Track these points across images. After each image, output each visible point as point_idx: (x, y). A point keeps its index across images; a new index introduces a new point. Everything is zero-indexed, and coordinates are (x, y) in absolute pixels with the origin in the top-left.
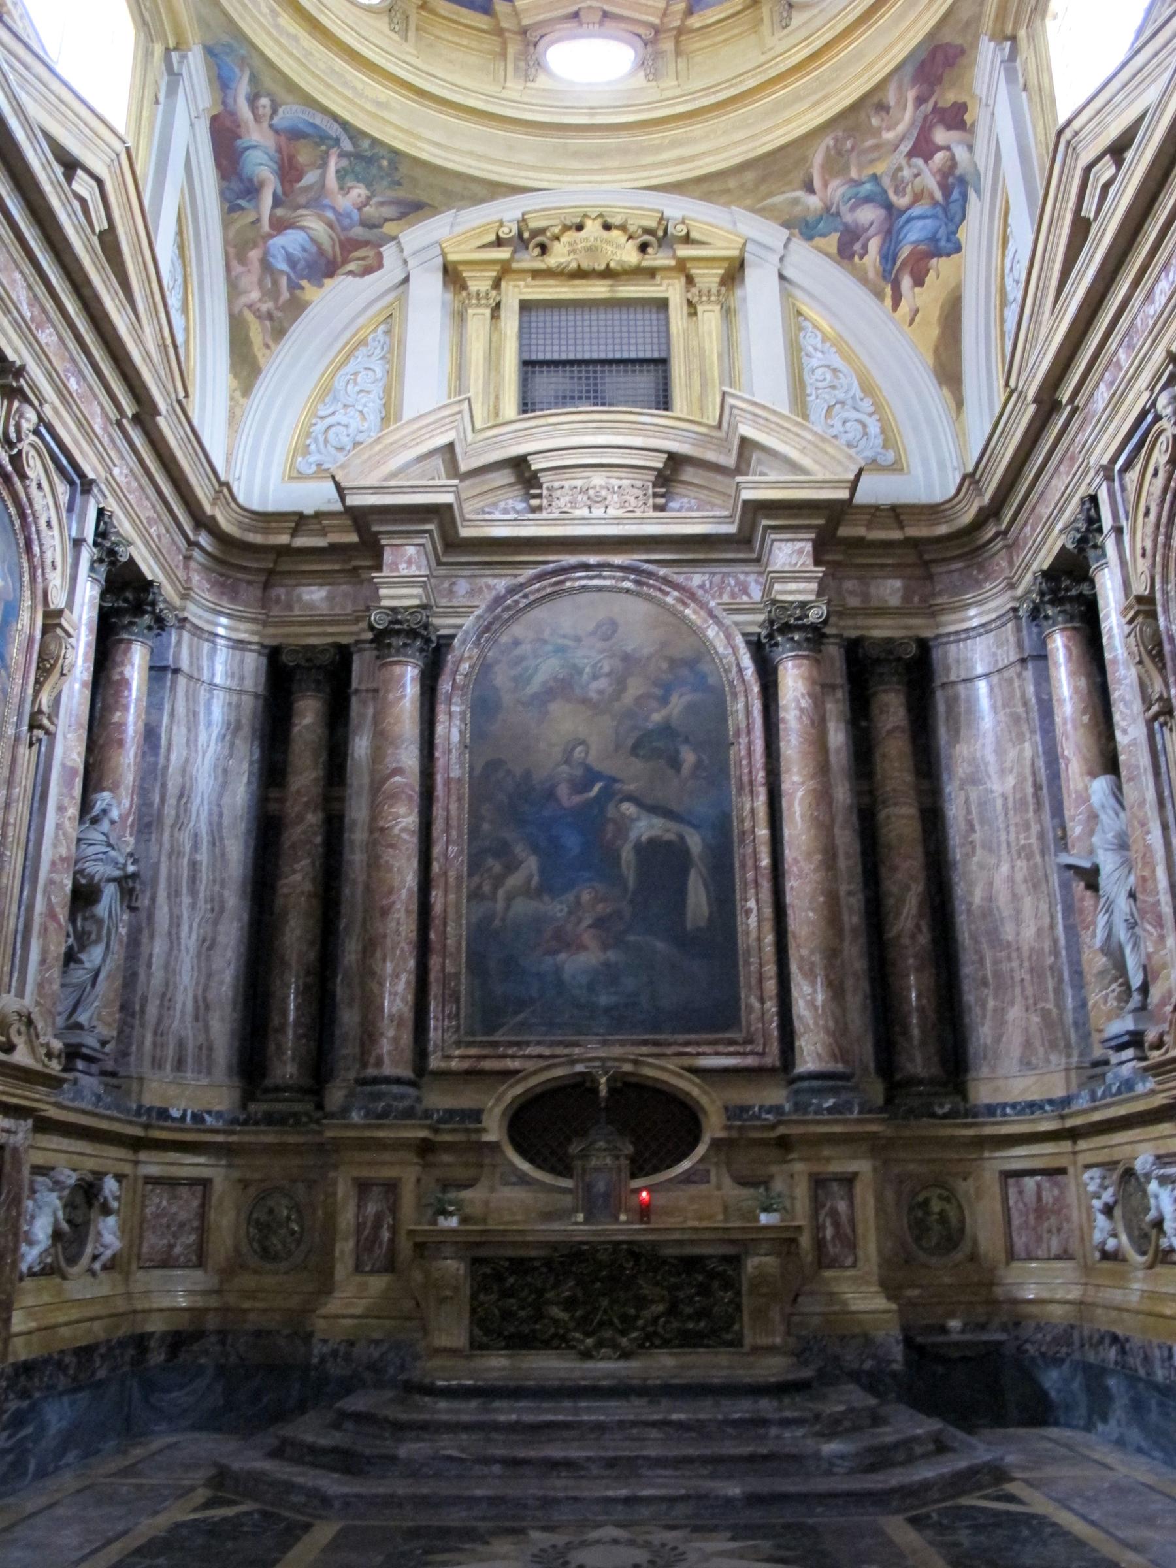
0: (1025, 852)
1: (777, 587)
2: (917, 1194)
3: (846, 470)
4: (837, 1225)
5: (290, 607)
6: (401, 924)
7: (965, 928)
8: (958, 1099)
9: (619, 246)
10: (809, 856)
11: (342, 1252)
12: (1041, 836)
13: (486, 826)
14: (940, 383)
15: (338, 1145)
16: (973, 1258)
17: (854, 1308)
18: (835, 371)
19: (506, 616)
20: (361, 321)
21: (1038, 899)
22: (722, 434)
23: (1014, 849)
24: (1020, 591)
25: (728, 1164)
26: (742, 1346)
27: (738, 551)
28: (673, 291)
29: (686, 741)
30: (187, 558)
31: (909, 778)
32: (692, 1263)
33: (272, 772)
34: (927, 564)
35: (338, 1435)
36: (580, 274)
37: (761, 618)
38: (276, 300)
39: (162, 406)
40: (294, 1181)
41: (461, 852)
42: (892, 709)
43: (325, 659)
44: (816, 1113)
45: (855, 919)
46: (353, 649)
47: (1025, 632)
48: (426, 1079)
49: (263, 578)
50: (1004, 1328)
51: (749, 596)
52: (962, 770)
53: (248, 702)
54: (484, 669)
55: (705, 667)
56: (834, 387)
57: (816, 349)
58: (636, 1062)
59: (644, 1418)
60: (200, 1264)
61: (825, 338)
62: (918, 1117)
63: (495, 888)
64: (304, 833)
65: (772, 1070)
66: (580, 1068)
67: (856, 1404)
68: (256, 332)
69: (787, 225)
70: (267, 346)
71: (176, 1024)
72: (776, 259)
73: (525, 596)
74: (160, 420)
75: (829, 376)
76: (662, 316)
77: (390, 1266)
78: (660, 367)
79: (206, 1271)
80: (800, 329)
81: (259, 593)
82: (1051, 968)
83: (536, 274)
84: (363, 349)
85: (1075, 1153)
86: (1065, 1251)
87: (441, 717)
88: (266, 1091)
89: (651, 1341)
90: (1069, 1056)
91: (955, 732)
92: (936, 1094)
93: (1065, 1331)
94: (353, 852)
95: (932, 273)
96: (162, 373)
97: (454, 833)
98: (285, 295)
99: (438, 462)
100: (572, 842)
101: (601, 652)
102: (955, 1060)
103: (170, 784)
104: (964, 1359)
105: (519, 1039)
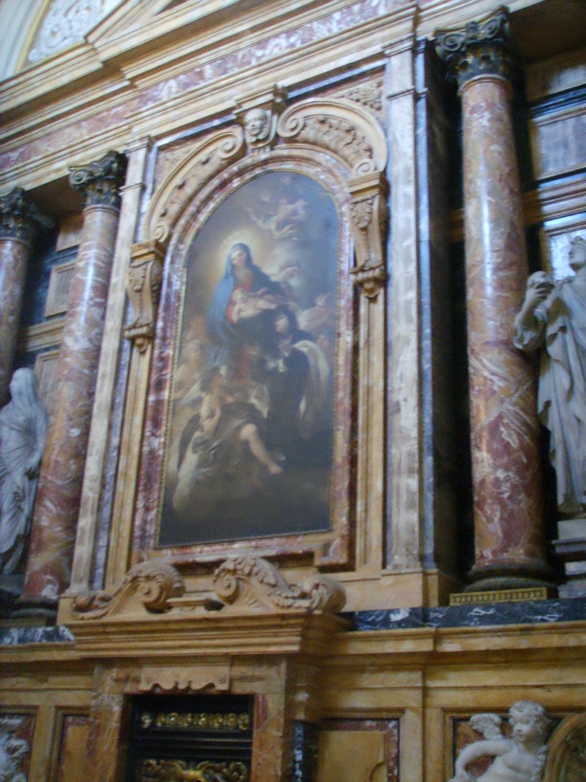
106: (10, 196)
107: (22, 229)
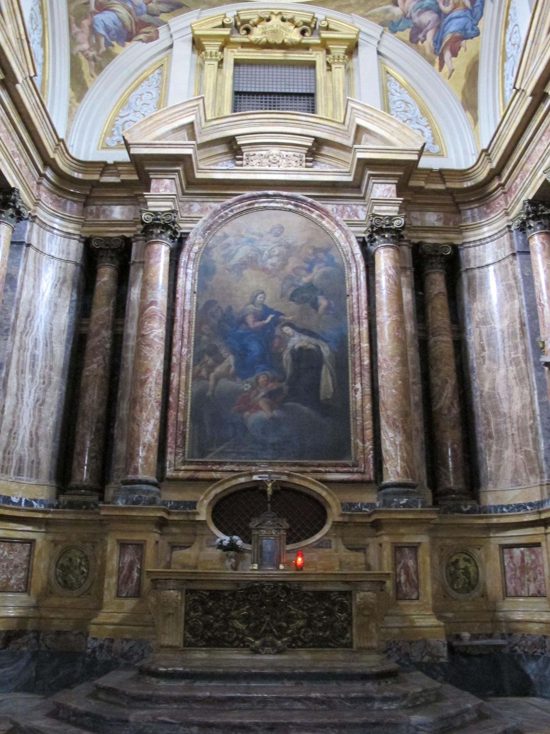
0: (515, 362)
1: (376, 208)
2: (451, 557)
3: (416, 144)
4: (407, 574)
5: (98, 216)
6: (153, 390)
7: (479, 405)
8: (474, 502)
9: (290, 31)
10: (392, 358)
11: (109, 584)
12: (525, 352)
13: (204, 338)
14: (465, 110)
15: (110, 519)
16: (484, 595)
17: (418, 624)
18: (406, 103)
19: (220, 221)
20: (145, 67)
21: (523, 388)
22: (345, 128)
23: (508, 360)
24: (512, 216)
25: (342, 537)
26: (352, 647)
27: (352, 192)
28: (319, 57)
29: (322, 294)
30: (39, 184)
31: (447, 321)
32: (323, 595)
33: (83, 308)
34: (457, 204)
35: (93, 702)
36: (268, 46)
37: (364, 229)
38: (98, 49)
39: (20, 78)
40: (84, 542)
41: (189, 352)
42: (437, 283)
43: (116, 245)
44: (396, 507)
45: (417, 398)
46: (133, 240)
47: (515, 240)
48: (164, 483)
49: (83, 200)
50: (503, 637)
51: (358, 217)
52: (477, 316)
53: (71, 268)
54: (207, 250)
55: (333, 253)
56: (406, 111)
57: (396, 91)
58: (289, 475)
59: (293, 695)
60: (26, 591)
61: (402, 86)
62: (454, 512)
63: (209, 373)
64: (100, 341)
65: (369, 482)
66: (255, 478)
67: (428, 687)
68: (86, 67)
69: (382, 24)
70: (92, 76)
71: (18, 447)
72: (375, 43)
73: (232, 211)
74: (18, 86)
75: (403, 105)
76: (312, 71)
77: (138, 594)
78: (310, 98)
79: (29, 595)
80: (388, 81)
81: (81, 208)
82: (531, 427)
83: (244, 45)
84: (146, 82)
85: (546, 534)
86: (539, 592)
87: (181, 274)
88: (71, 489)
89: (296, 643)
90: (542, 478)
91: (473, 296)
92: (462, 499)
93: (540, 640)
94: (127, 353)
95: (462, 49)
96: (20, 57)
97: (186, 341)
98: (103, 49)
99: (184, 133)
100: (255, 348)
101: (274, 243)
102: (473, 479)
103: (21, 309)
104: (481, 656)
105: (221, 460)
106: (523, 208)
107: (540, 223)
